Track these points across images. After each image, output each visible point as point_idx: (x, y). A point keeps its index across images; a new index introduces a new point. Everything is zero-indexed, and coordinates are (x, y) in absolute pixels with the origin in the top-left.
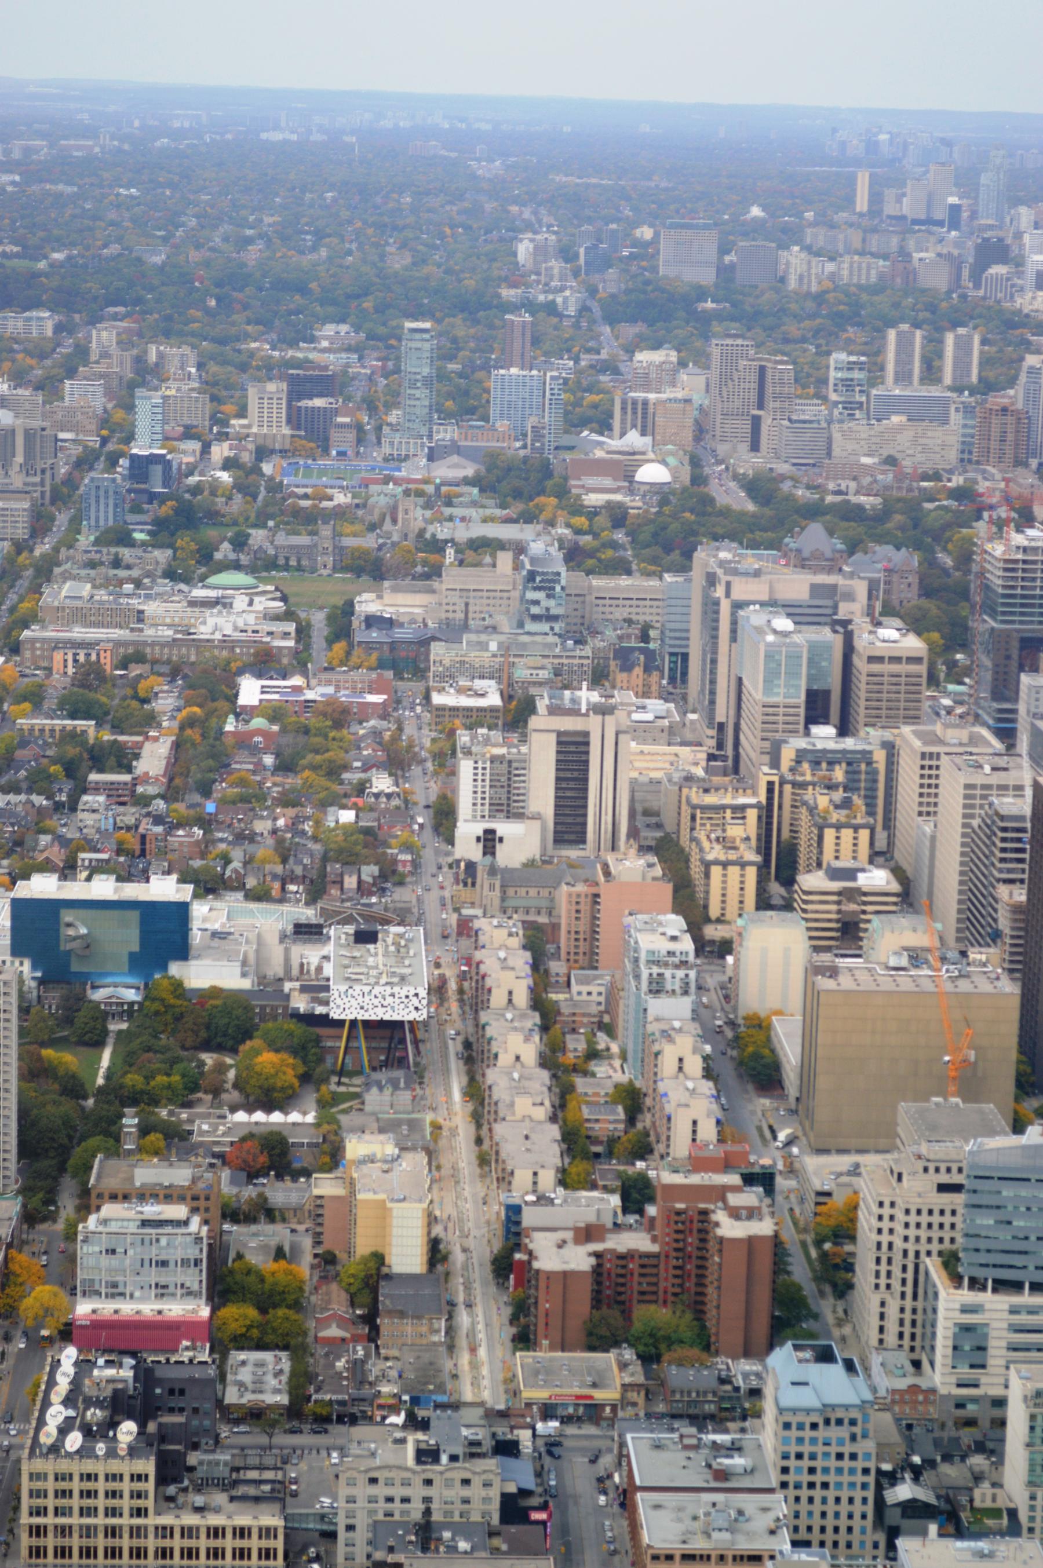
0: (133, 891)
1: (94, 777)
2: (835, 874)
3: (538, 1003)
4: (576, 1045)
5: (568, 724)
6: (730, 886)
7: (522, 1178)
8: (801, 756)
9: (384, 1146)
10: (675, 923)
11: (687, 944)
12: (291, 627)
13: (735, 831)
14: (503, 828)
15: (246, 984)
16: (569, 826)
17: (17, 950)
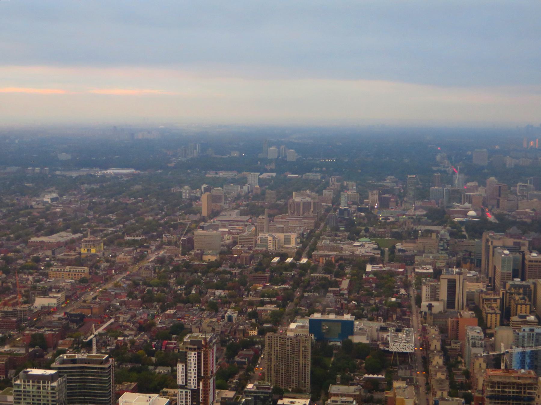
0: (339, 318)
1: (330, 289)
2: (521, 317)
3: (443, 348)
4: (452, 361)
5: (451, 277)
6: (493, 319)
7: (439, 393)
8: (512, 286)
9: (403, 384)
10: (479, 329)
11: (482, 335)
12: (380, 252)
13: (494, 305)
14: (434, 303)
15: (368, 342)
16: (451, 303)
17: (310, 332)
